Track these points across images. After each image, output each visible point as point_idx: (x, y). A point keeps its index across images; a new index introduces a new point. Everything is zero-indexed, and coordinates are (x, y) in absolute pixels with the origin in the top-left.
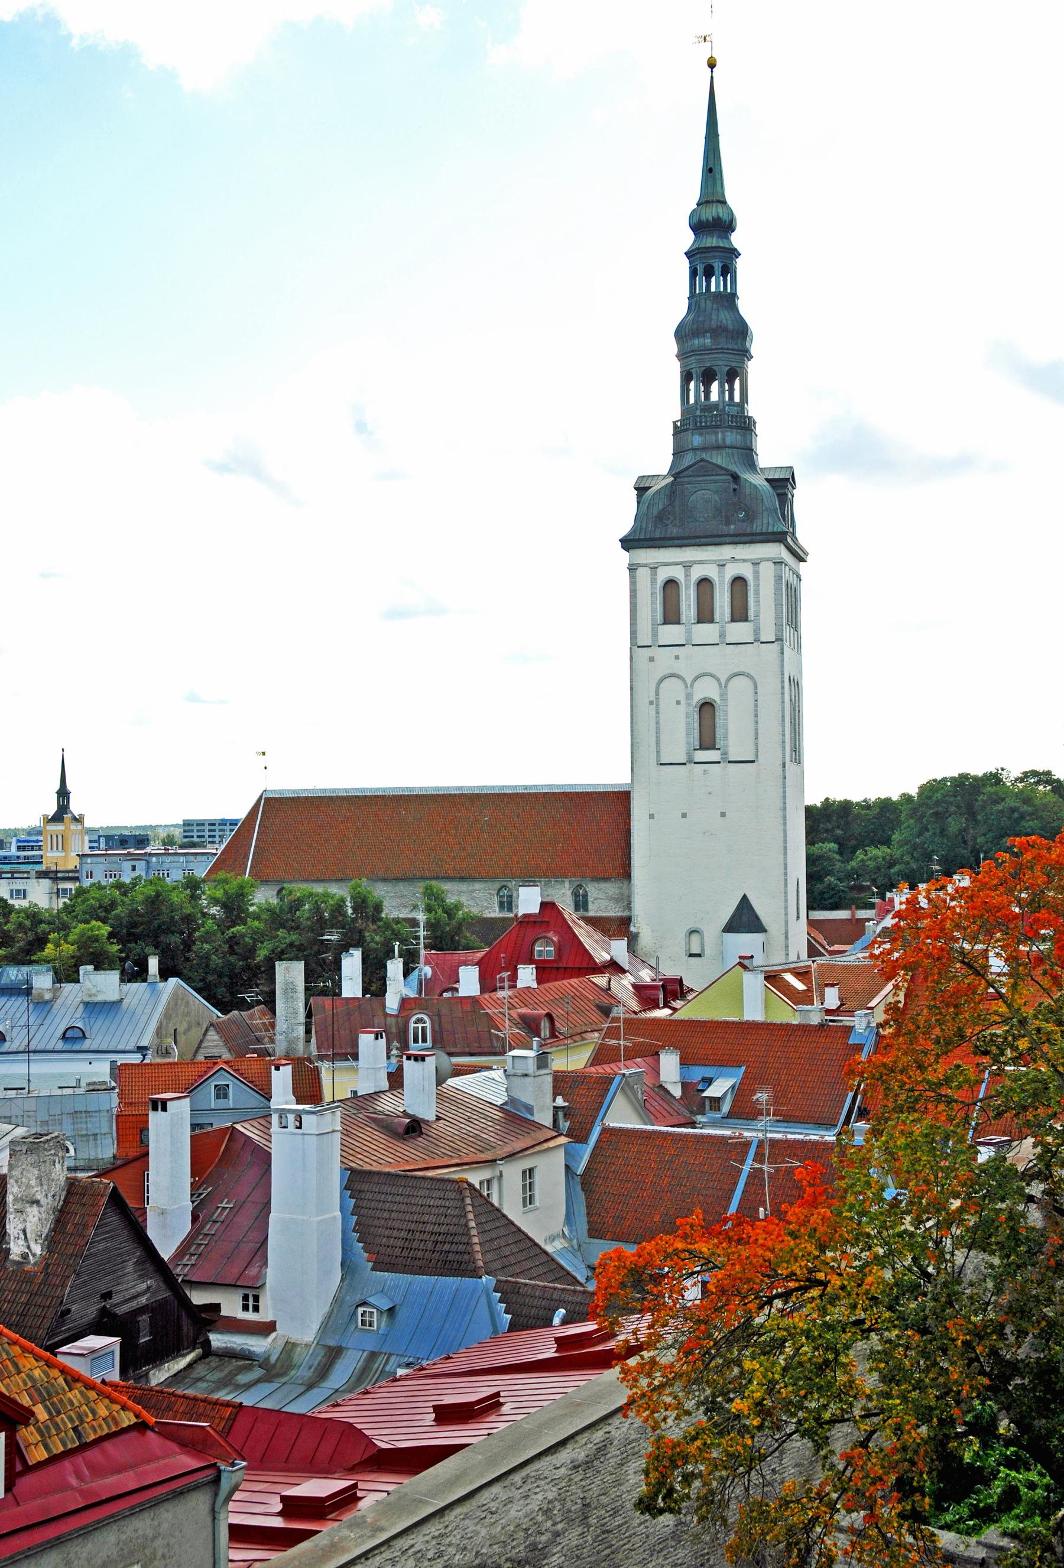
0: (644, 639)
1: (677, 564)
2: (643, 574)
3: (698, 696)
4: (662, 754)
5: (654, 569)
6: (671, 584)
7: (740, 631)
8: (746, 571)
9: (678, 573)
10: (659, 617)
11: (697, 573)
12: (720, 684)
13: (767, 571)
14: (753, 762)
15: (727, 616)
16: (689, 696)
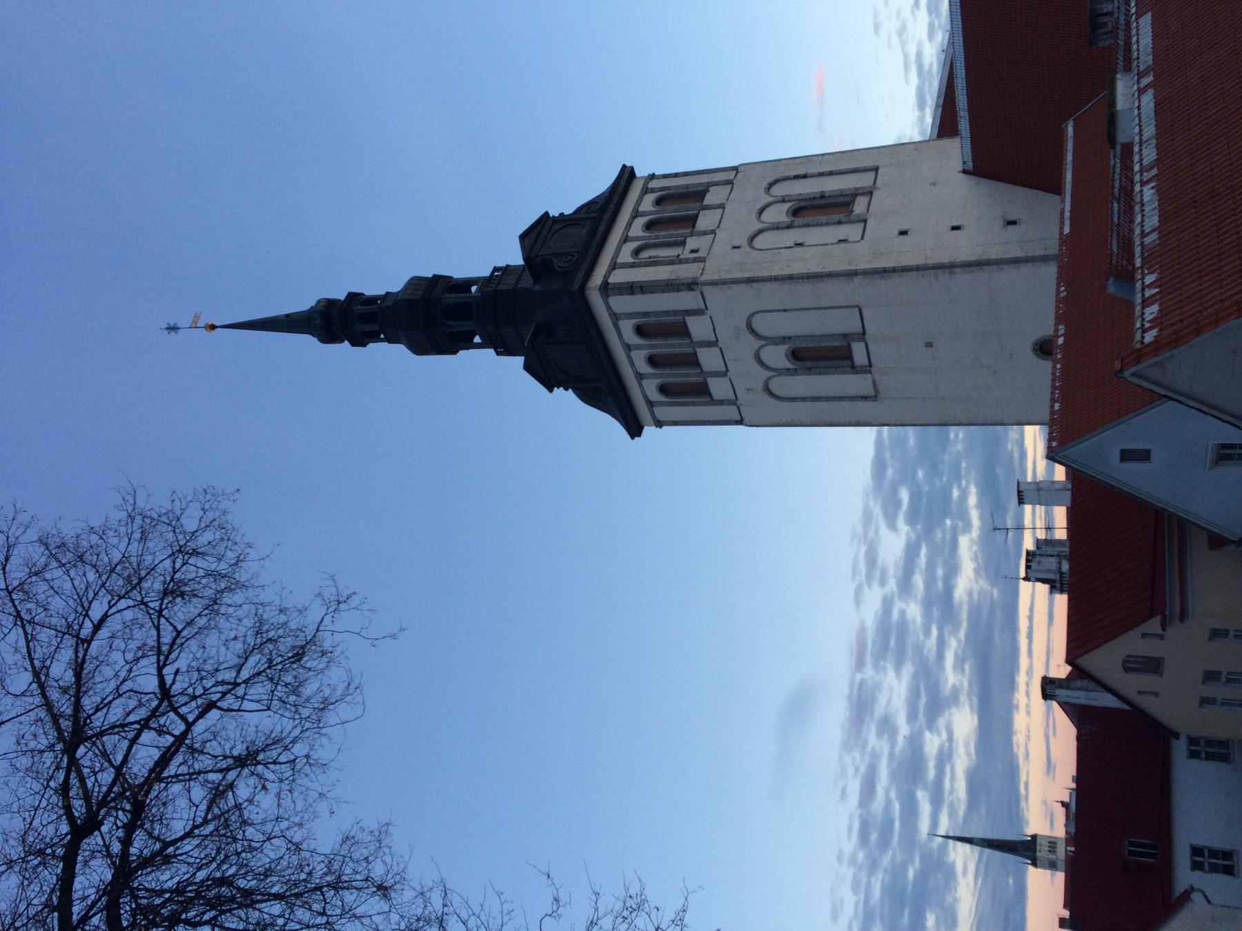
0: (731, 412)
1: (641, 385)
2: (661, 412)
3: (787, 364)
4: (865, 393)
5: (651, 404)
6: (663, 389)
7: (698, 328)
8: (627, 326)
9: (651, 387)
10: (702, 399)
11: (644, 368)
12: (763, 346)
13: (620, 303)
14: (860, 310)
15: (687, 341)
16: (788, 372)
